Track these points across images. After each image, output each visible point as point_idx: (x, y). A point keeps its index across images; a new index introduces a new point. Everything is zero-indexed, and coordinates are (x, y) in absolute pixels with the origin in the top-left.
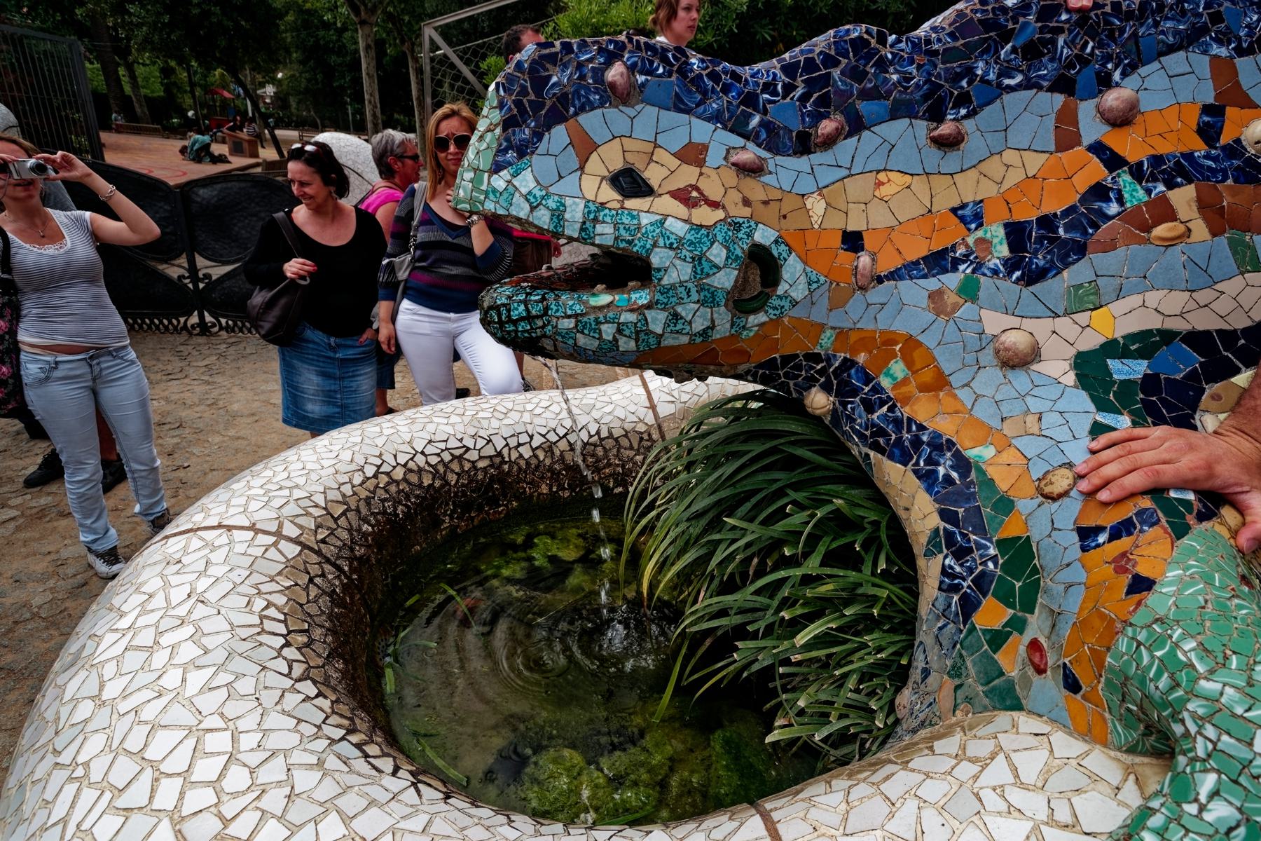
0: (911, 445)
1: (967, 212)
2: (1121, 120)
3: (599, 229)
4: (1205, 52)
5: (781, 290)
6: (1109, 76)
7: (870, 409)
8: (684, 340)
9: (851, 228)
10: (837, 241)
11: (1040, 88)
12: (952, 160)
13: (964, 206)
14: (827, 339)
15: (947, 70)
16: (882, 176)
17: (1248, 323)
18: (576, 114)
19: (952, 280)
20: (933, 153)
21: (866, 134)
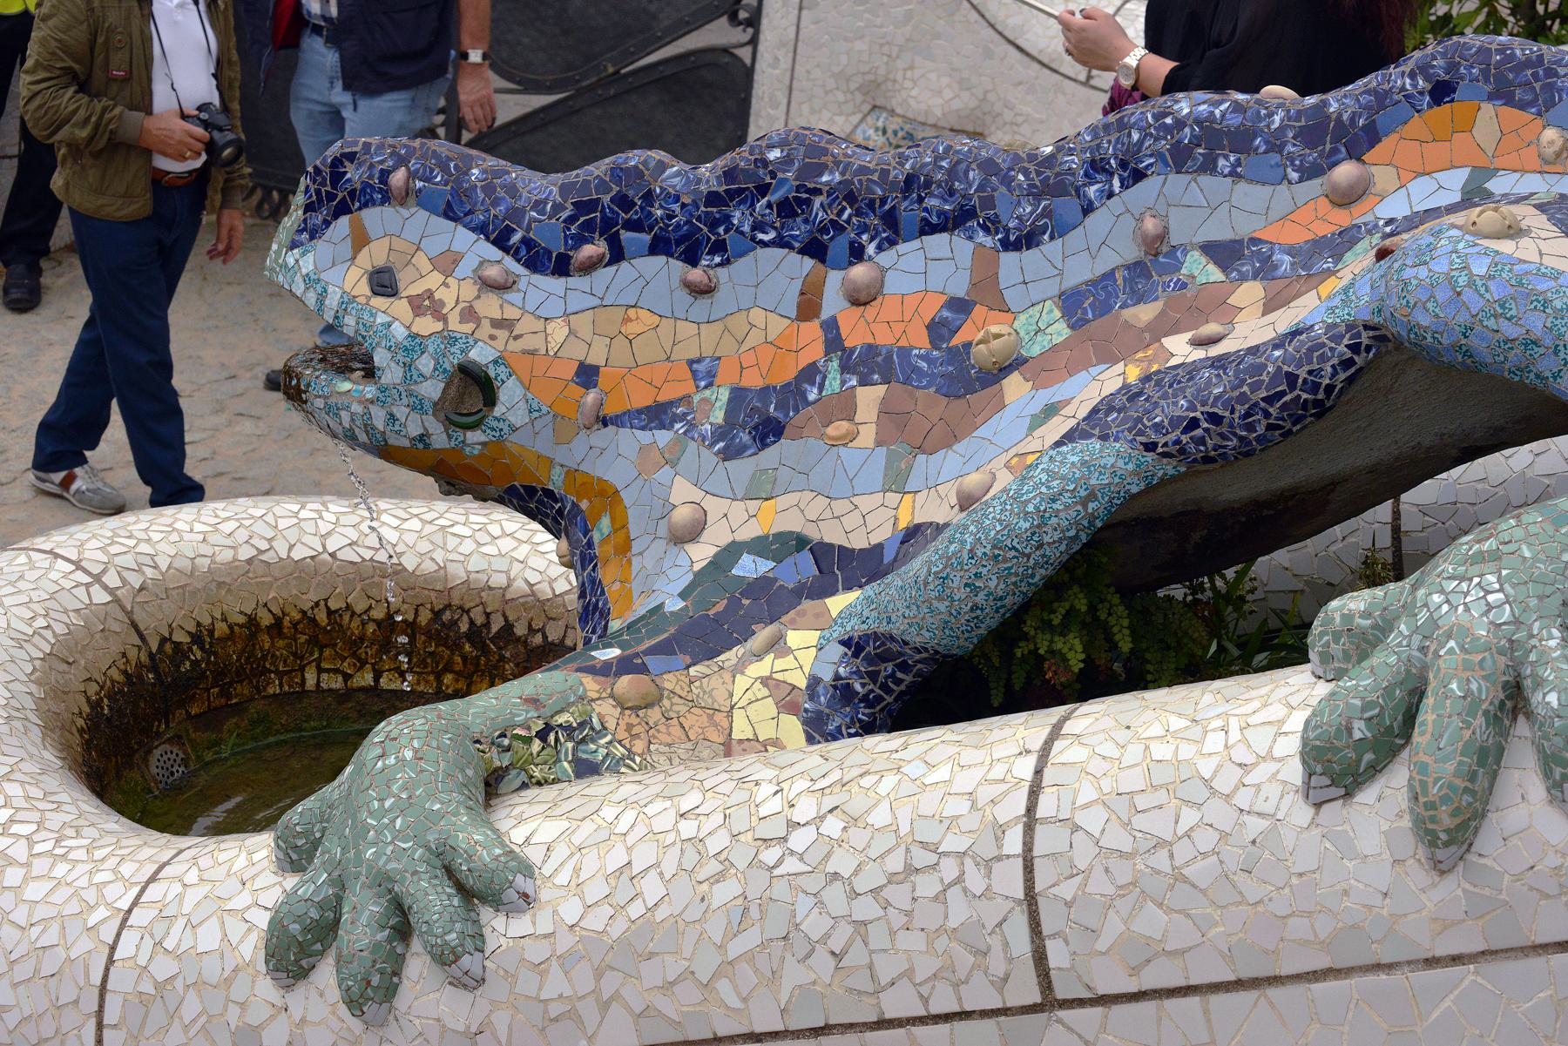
4: (970, 238)
5: (498, 410)
6: (862, 248)
9: (588, 362)
11: (792, 248)
12: (702, 306)
15: (707, 213)
16: (632, 312)
17: (866, 545)
18: (360, 209)
20: (684, 296)
21: (624, 265)
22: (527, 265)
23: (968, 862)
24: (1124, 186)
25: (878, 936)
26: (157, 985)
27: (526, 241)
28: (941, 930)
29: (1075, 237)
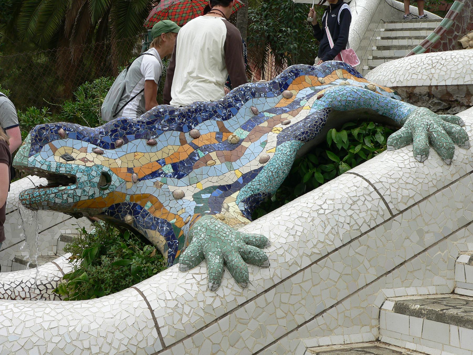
0: (156, 224)
1: (160, 161)
2: (196, 137)
3: (61, 169)
4: (214, 120)
5: (112, 183)
6: (191, 126)
7: (144, 218)
8: (87, 198)
10: (126, 171)
11: (174, 130)
13: (159, 160)
14: (128, 198)
16: (136, 153)
18: (51, 141)
19: (159, 179)
20: (148, 147)
21: (129, 143)
22: (103, 148)
23: (365, 196)
24: (244, 103)
25: (355, 217)
26: (172, 309)
27: (101, 142)
28: (367, 210)
29: (238, 115)
